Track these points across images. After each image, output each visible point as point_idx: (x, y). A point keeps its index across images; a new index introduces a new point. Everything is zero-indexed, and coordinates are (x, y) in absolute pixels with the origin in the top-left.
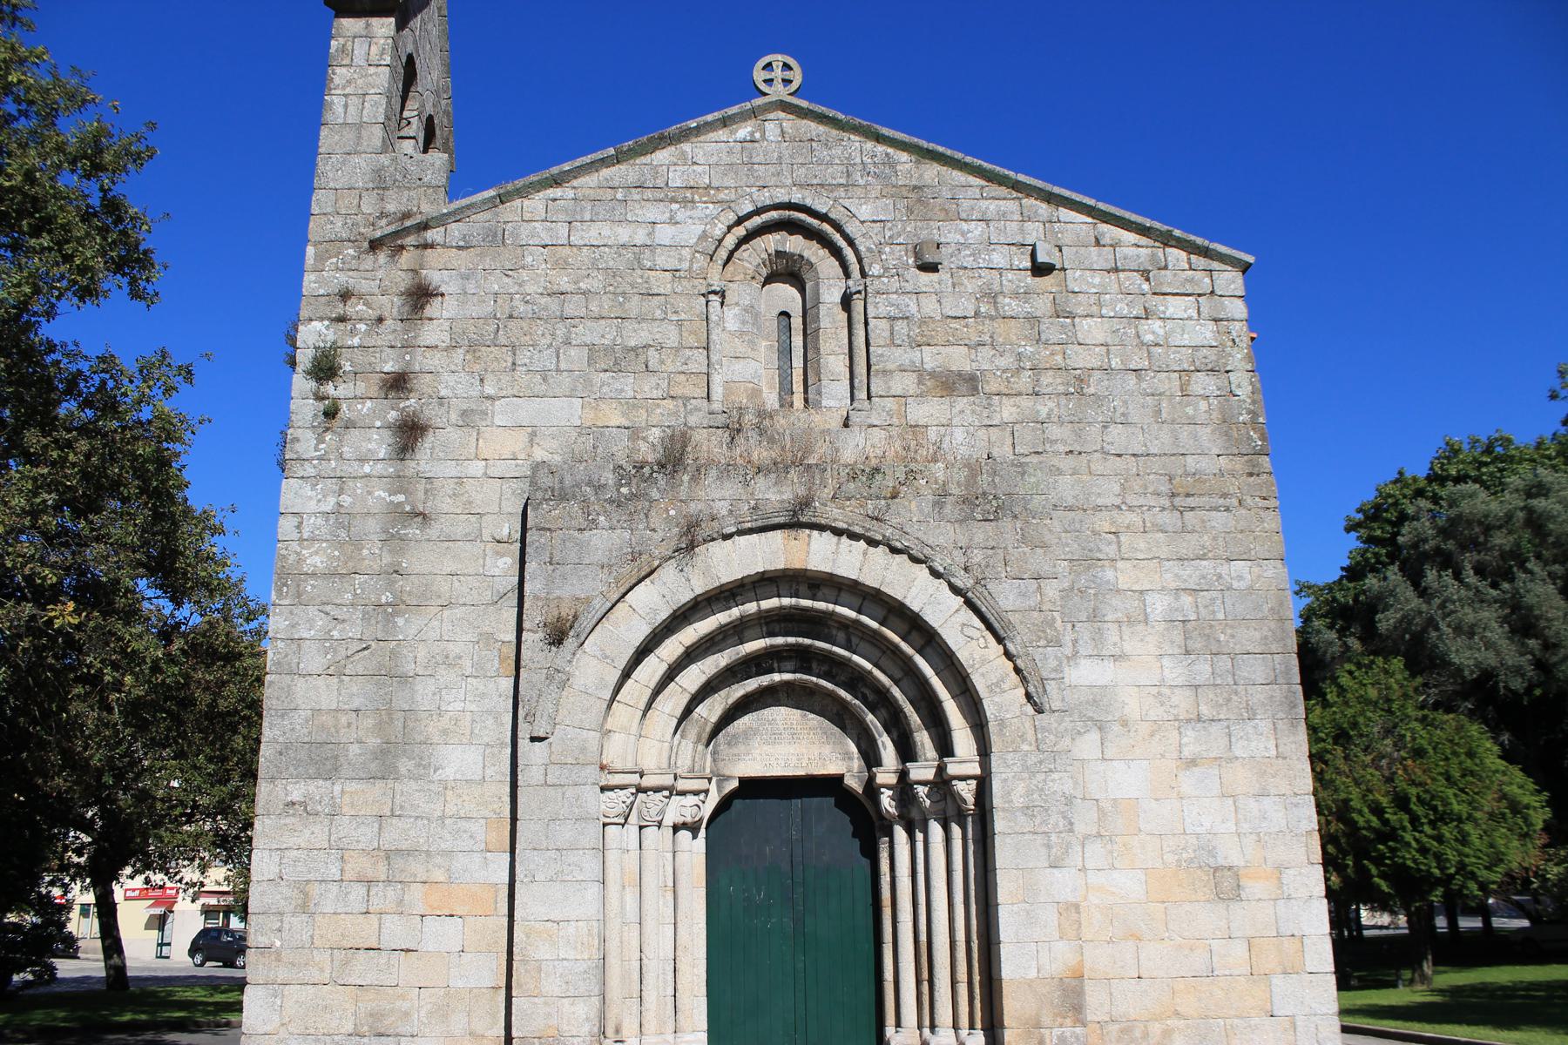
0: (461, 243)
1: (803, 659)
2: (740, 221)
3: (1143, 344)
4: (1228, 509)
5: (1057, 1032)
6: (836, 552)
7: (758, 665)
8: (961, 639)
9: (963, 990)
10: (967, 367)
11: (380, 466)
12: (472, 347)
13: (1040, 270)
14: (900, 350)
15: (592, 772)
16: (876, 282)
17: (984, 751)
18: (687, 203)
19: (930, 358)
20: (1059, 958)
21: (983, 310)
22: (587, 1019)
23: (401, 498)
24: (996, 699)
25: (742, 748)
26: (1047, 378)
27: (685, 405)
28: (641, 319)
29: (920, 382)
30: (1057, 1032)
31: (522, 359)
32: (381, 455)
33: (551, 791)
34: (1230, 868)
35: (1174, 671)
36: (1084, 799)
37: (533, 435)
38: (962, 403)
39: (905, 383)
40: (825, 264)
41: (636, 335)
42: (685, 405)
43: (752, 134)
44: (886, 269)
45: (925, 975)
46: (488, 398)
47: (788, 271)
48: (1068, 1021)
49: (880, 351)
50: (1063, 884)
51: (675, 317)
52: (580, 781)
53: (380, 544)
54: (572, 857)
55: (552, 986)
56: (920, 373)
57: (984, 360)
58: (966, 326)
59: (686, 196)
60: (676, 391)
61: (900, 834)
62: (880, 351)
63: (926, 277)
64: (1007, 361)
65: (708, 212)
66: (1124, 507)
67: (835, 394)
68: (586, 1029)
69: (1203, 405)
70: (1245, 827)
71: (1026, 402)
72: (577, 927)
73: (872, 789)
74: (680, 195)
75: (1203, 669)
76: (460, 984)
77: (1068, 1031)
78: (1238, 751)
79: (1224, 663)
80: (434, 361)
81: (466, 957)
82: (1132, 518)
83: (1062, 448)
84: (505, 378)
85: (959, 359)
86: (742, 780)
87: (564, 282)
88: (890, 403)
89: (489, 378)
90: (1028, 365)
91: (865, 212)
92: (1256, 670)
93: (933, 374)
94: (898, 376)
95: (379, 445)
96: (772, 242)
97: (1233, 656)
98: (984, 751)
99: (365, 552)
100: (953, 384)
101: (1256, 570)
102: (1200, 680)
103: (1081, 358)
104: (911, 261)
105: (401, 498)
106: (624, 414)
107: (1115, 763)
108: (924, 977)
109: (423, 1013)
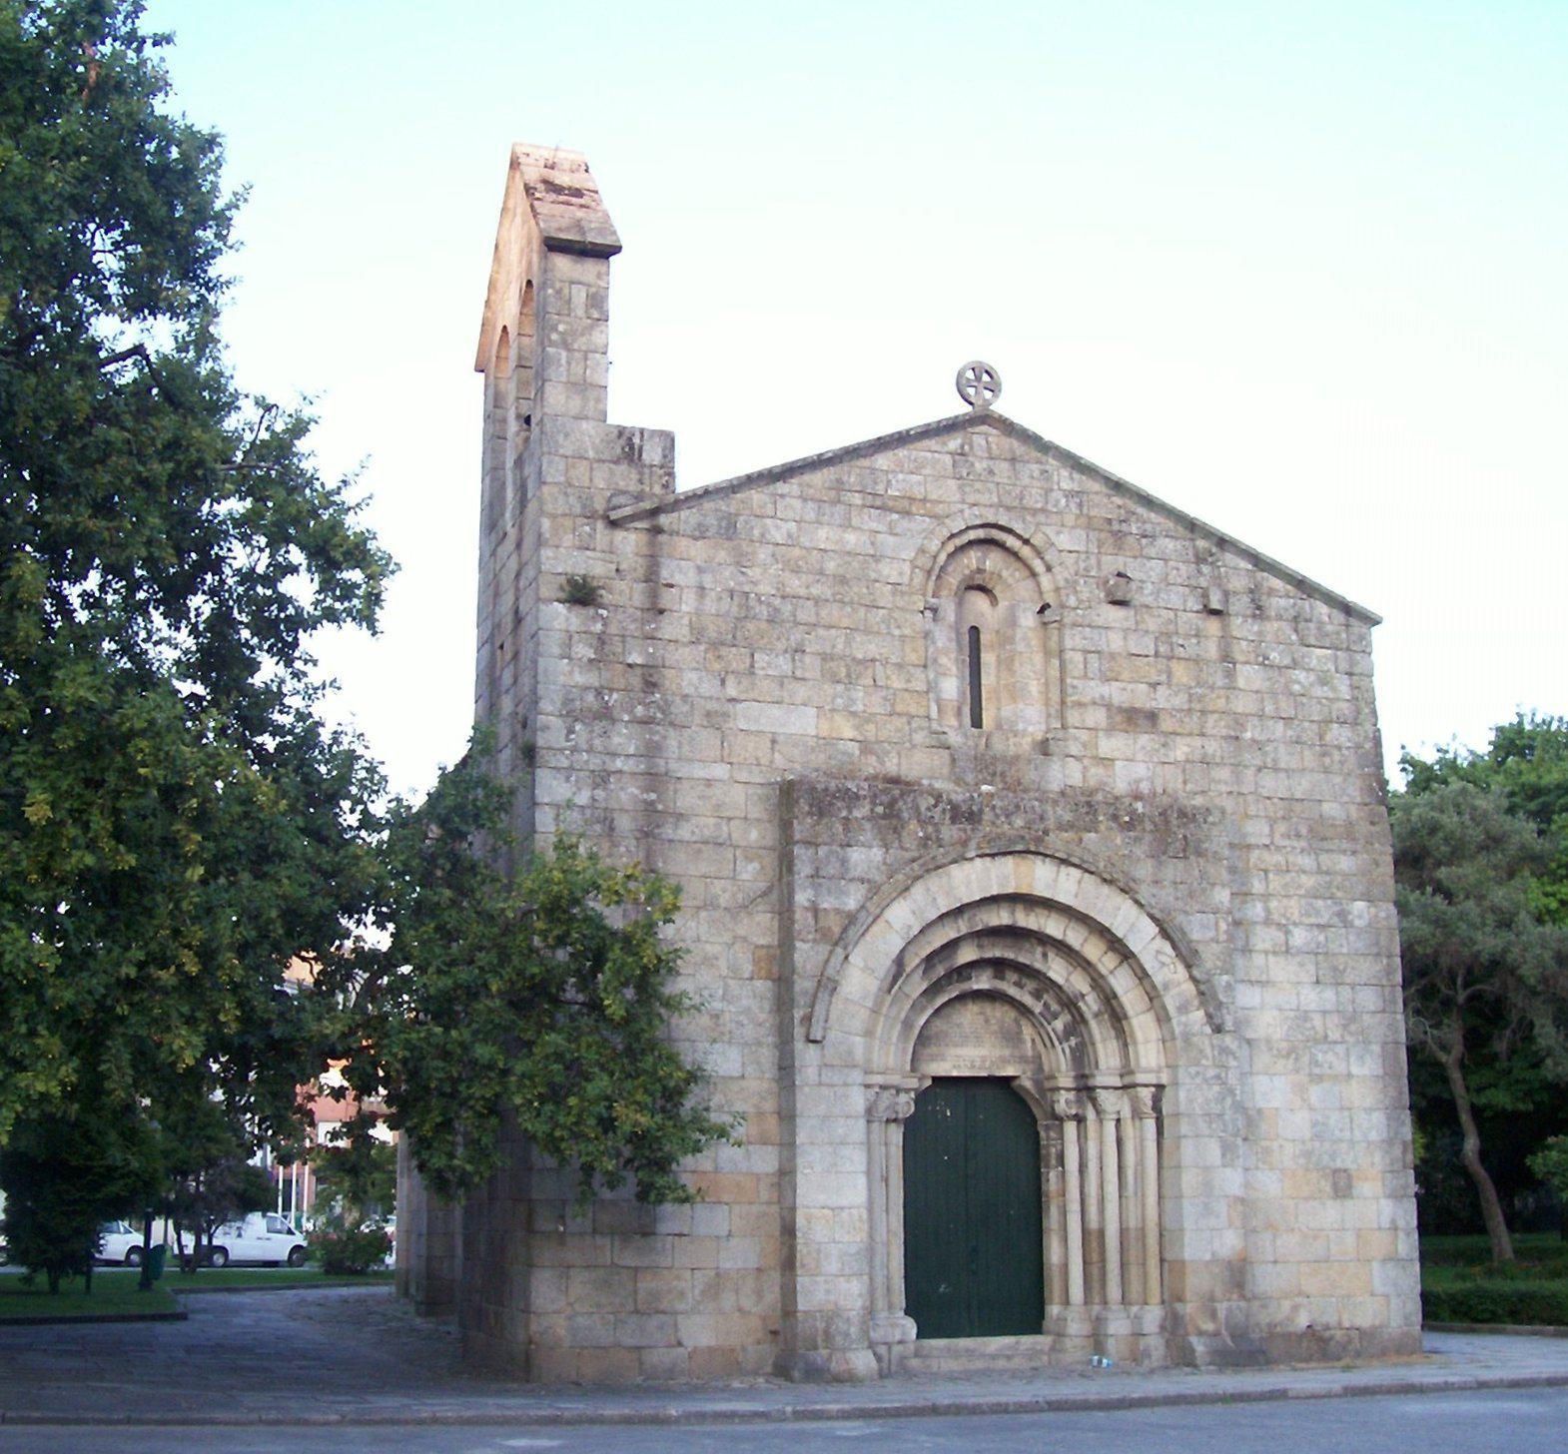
0: (697, 533)
1: (999, 966)
2: (952, 536)
3: (1291, 694)
4: (1354, 853)
5: (1225, 1305)
6: (1055, 880)
8: (1156, 964)
10: (1149, 705)
11: (631, 762)
12: (715, 645)
14: (1092, 683)
15: (857, 1076)
16: (1072, 614)
18: (907, 513)
19: (1117, 693)
20: (1229, 1243)
21: (1162, 649)
22: (860, 1295)
23: (653, 796)
24: (1183, 1019)
25: (933, 1050)
26: (1211, 719)
27: (909, 723)
28: (867, 631)
29: (1109, 717)
30: (1225, 1305)
32: (632, 750)
33: (825, 1091)
34: (1345, 1171)
37: (774, 742)
38: (1144, 739)
39: (1097, 717)
41: (865, 648)
42: (909, 723)
44: (1081, 601)
45: (1095, 1257)
48: (1235, 1296)
49: (1075, 682)
51: (897, 632)
52: (850, 1081)
53: (634, 842)
54: (846, 1151)
55: (833, 1266)
57: (1162, 699)
58: (1148, 664)
59: (906, 506)
60: (899, 708)
62: (1075, 682)
63: (1115, 614)
64: (1180, 701)
65: (925, 526)
68: (859, 1303)
69: (1337, 756)
70: (1358, 1135)
71: (1197, 742)
72: (850, 1214)
74: (900, 504)
75: (1329, 994)
76: (728, 1265)
77: (1234, 1304)
78: (1355, 1070)
79: (1346, 992)
81: (734, 1241)
82: (1278, 858)
83: (1224, 788)
84: (745, 682)
85: (1140, 696)
86: (935, 1079)
88: (1084, 736)
89: (731, 681)
90: (1198, 707)
91: (1064, 541)
92: (1369, 999)
93: (1120, 710)
94: (1091, 710)
95: (629, 738)
96: (972, 558)
97: (1353, 986)
99: (622, 849)
100: (1136, 719)
101: (1373, 910)
102: (1328, 1007)
103: (1243, 704)
104: (1102, 595)
105: (653, 796)
106: (857, 728)
107: (1261, 1077)
109: (697, 1292)
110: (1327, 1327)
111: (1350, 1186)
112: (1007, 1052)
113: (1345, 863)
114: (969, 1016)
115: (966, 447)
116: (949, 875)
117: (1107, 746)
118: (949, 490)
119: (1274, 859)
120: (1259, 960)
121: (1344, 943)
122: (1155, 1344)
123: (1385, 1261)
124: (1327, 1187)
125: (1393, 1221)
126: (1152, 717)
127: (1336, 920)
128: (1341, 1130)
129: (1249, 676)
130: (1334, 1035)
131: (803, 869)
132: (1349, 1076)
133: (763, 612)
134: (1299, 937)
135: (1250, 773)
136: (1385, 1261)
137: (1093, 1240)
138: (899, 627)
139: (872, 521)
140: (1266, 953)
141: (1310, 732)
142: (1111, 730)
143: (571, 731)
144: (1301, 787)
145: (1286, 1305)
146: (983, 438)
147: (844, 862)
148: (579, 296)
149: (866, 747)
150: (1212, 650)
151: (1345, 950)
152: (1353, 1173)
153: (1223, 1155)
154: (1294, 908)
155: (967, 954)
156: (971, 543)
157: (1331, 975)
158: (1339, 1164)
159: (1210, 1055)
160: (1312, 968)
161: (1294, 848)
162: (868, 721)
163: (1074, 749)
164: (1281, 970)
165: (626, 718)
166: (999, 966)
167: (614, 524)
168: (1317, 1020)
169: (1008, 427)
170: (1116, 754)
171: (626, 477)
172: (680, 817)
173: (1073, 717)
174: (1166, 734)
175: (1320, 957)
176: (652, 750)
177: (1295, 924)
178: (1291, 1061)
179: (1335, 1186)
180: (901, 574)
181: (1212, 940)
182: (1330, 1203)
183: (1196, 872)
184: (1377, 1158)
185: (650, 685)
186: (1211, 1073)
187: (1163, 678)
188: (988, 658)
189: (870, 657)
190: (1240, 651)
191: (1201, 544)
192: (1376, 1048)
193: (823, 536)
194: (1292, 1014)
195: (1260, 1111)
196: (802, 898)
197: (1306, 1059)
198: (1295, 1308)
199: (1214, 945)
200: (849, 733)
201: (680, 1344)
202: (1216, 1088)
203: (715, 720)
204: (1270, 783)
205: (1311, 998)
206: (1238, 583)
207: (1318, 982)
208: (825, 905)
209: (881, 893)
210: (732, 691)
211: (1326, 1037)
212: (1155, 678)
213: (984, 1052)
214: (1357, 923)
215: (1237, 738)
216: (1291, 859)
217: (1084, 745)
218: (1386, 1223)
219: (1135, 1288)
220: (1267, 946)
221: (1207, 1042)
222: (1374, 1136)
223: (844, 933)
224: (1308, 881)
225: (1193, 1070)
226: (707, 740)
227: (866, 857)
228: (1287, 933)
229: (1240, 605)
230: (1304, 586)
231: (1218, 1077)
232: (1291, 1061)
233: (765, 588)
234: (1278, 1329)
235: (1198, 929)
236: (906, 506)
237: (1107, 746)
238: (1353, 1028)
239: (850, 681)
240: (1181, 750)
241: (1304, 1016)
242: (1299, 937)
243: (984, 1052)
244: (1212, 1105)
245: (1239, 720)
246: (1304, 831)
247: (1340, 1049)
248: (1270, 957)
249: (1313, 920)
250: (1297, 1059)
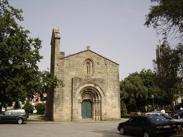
1: (89, 91)
9: (98, 114)
13: (106, 65)
17: (101, 99)
20: (105, 112)
31: (71, 69)
40: (91, 63)
41: (79, 68)
47: (88, 63)
50: (105, 107)
59: (82, 57)
61: (94, 103)
63: (98, 65)
67: (91, 72)
73: (93, 100)
80: (65, 69)
85: (100, 71)
87: (74, 63)
98: (101, 99)
100: (99, 73)
108: (96, 113)
113: (116, 83)
114: (87, 95)
118: (86, 56)
119: (110, 83)
121: (115, 89)
122: (100, 119)
124: (113, 107)
126: (101, 73)
129: (109, 69)
131: (73, 85)
133: (71, 65)
134: (112, 89)
137: (96, 111)
139: (79, 58)
141: (113, 73)
146: (88, 52)
148: (58, 42)
154: (111, 87)
155: (86, 90)
157: (114, 91)
163: (95, 75)
164: (110, 91)
166: (89, 91)
167: (60, 59)
169: (90, 51)
171: (62, 56)
173: (95, 73)
188: (88, 68)
190: (108, 67)
191: (105, 59)
192: (117, 97)
193: (75, 60)
196: (73, 86)
203: (67, 74)
204: (110, 77)
206: (108, 62)
209: (79, 87)
218: (118, 110)
222: (117, 104)
223: (77, 89)
226: (67, 75)
227: (78, 84)
229: (108, 64)
235: (103, 89)
236: (82, 57)
239: (78, 70)
241: (112, 95)
242: (112, 89)
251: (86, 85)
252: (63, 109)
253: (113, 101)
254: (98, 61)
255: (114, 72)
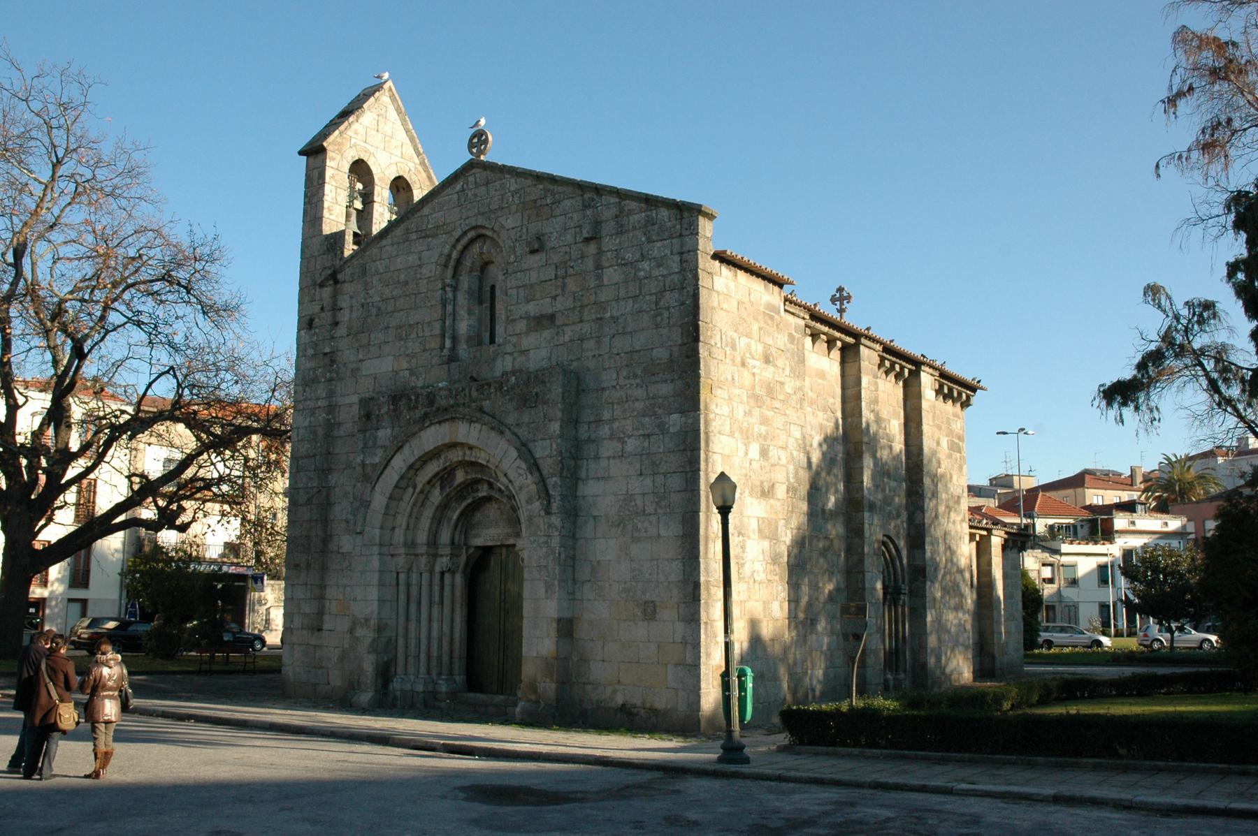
4: (672, 381)
6: (469, 432)
7: (472, 488)
14: (521, 306)
18: (435, 236)
19: (532, 309)
24: (529, 507)
34: (652, 602)
35: (637, 486)
36: (585, 561)
37: (375, 378)
38: (547, 334)
39: (521, 326)
43: (463, 186)
46: (361, 361)
48: (548, 680)
56: (528, 317)
66: (618, 387)
75: (648, 482)
78: (663, 532)
97: (665, 475)
100: (544, 321)
107: (601, 540)
110: (635, 706)
111: (654, 612)
112: (510, 530)
115: (465, 186)
116: (420, 438)
117: (528, 342)
120: (603, 463)
123: (676, 665)
125: (684, 637)
126: (552, 318)
127: (657, 430)
128: (650, 574)
129: (612, 275)
130: (650, 509)
132: (659, 536)
133: (374, 311)
134: (631, 445)
135: (606, 340)
136: (676, 665)
138: (429, 301)
140: (609, 458)
142: (529, 331)
143: (305, 391)
144: (640, 341)
145: (609, 690)
147: (376, 438)
149: (412, 372)
150: (590, 263)
151: (661, 450)
152: (657, 603)
153: (546, 592)
154: (629, 425)
156: (472, 242)
158: (648, 597)
159: (543, 529)
160: (638, 466)
161: (632, 385)
162: (413, 357)
165: (323, 380)
168: (639, 502)
170: (531, 347)
172: (339, 424)
174: (559, 327)
175: (644, 457)
176: (331, 394)
177: (629, 437)
178: (621, 528)
179: (645, 612)
180: (431, 271)
181: (548, 456)
182: (640, 623)
183: (542, 414)
184: (675, 592)
185: (333, 362)
186: (542, 540)
187: (559, 291)
189: (416, 321)
194: (622, 497)
195: (598, 562)
197: (630, 527)
198: (614, 692)
199: (548, 459)
200: (405, 366)
201: (329, 684)
202: (545, 549)
203: (355, 372)
204: (620, 343)
205: (636, 486)
206: (608, 214)
207: (641, 474)
208: (367, 462)
210: (361, 357)
211: (644, 511)
212: (554, 293)
213: (498, 531)
214: (672, 430)
215: (601, 319)
216: (629, 392)
217: (515, 346)
218: (678, 638)
219: (411, 669)
220: (610, 453)
221: (541, 521)
222: (673, 578)
224: (639, 406)
225: (532, 539)
228: (624, 443)
230: (650, 201)
231: (546, 542)
232: (621, 528)
233: (376, 298)
234: (603, 704)
237: (526, 342)
238: (663, 503)
240: (568, 333)
241: (629, 497)
243: (498, 531)
244: (542, 560)
245: (602, 306)
246: (639, 373)
247: (653, 518)
248: (611, 461)
249: (641, 432)
250: (624, 527)
251: (431, 437)
252: (326, 617)
253: (635, 550)
254: (535, 227)
255: (653, 287)
